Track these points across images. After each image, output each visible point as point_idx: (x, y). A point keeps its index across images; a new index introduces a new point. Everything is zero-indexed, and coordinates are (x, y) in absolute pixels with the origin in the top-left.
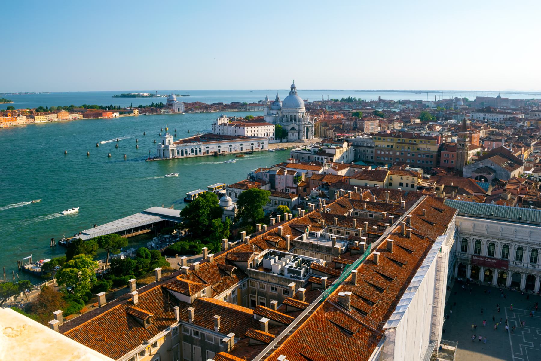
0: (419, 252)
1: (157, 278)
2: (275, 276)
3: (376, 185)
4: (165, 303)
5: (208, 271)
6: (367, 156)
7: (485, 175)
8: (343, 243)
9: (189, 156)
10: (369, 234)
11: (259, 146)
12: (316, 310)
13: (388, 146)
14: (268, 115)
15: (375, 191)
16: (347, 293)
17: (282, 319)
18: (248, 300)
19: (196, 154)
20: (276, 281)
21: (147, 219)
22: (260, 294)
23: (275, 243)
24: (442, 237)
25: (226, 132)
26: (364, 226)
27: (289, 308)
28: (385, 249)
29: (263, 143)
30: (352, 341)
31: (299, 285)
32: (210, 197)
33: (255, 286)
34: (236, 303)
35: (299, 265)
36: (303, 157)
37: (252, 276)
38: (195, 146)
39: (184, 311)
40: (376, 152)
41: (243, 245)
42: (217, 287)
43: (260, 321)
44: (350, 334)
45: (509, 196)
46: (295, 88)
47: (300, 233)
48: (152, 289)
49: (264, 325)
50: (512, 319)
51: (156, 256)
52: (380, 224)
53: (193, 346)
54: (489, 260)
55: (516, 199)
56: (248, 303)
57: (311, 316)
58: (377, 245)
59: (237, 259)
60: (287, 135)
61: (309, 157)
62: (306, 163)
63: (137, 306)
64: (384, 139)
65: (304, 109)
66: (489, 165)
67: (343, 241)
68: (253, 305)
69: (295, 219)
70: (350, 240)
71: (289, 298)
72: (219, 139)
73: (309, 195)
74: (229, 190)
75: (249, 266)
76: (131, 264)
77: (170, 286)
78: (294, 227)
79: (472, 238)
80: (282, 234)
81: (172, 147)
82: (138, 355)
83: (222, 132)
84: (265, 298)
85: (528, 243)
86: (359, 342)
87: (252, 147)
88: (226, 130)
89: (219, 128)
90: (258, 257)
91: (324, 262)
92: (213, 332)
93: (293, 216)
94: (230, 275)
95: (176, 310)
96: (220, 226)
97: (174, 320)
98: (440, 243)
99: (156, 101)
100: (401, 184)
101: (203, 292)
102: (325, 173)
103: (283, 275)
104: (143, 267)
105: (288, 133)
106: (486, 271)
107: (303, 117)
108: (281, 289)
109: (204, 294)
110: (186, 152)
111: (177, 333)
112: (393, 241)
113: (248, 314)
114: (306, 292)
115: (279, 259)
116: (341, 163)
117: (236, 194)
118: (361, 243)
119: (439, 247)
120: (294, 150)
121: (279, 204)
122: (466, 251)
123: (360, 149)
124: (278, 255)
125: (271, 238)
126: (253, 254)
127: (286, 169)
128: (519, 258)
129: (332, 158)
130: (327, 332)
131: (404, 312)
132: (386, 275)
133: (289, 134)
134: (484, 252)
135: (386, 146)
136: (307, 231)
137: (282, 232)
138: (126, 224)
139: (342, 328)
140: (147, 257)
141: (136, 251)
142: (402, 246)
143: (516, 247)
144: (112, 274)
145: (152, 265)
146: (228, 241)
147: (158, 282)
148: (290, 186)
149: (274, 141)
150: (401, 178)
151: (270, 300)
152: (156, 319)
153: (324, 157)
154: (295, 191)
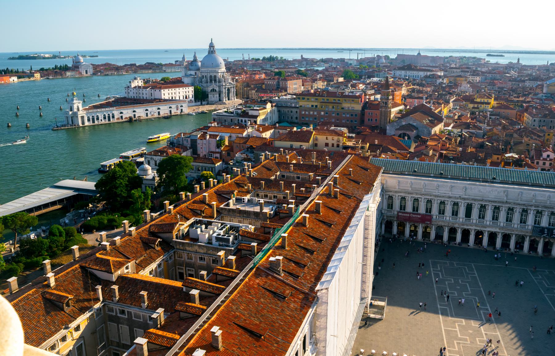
0: (347, 211)
1: (74, 257)
2: (203, 246)
3: (302, 146)
4: (85, 283)
5: (130, 246)
6: (292, 117)
7: (407, 133)
8: (271, 207)
9: (100, 122)
10: (297, 196)
11: (177, 109)
12: (248, 277)
13: (312, 106)
14: (186, 75)
15: (301, 152)
16: (278, 257)
17: (213, 289)
18: (176, 273)
19: (109, 120)
20: (205, 250)
21: (58, 194)
22: (189, 265)
23: (201, 211)
24: (369, 195)
25: (141, 95)
26: (291, 188)
27: (219, 278)
28: (314, 211)
29: (182, 106)
30: (285, 305)
31: (228, 253)
32: (128, 167)
33: (182, 258)
34: (163, 276)
35: (227, 232)
36: (225, 120)
37: (178, 247)
38: (107, 111)
39: (107, 290)
40: (300, 112)
41: (167, 215)
42: (141, 261)
43: (190, 293)
44: (283, 298)
45: (431, 152)
46: (213, 47)
47: (226, 199)
48: (69, 270)
49: (195, 297)
50: (436, 271)
51: (71, 234)
52: (307, 185)
53: (120, 325)
54: (414, 216)
55: (437, 155)
56: (176, 276)
57: (242, 284)
58: (306, 207)
59: (161, 231)
60: (208, 97)
61: (231, 119)
62: (229, 126)
63: (54, 289)
64: (308, 99)
65: (223, 69)
66: (411, 123)
67: (271, 205)
68: (181, 277)
69: (221, 185)
70: (278, 204)
71: (219, 267)
72: (134, 103)
73: (233, 159)
74: (148, 158)
75: (175, 237)
76: (44, 244)
77: (89, 265)
78: (220, 193)
79: (397, 195)
80: (207, 202)
81: (81, 113)
82: (59, 341)
83: (137, 95)
84: (194, 269)
85: (450, 197)
86: (292, 305)
87: (170, 111)
88: (141, 93)
89: (132, 91)
90: (184, 227)
91: (253, 227)
92: (140, 309)
93: (218, 183)
94: (154, 248)
95: (98, 289)
96: (140, 197)
97: (97, 300)
98: (368, 201)
99: (59, 63)
100: (327, 145)
101: (127, 268)
102: (249, 135)
103: (211, 243)
104: (57, 246)
105: (208, 95)
106: (411, 226)
108: (210, 259)
109: (127, 271)
110: (98, 119)
111: (101, 314)
112: (321, 202)
113: (177, 287)
114: (236, 260)
115: (206, 228)
116: (265, 125)
117: (156, 162)
118: (290, 206)
119: (366, 206)
120: (215, 112)
121: (202, 171)
122: (392, 208)
123: (284, 109)
124: (204, 224)
125: (196, 206)
126: (178, 224)
127: (208, 133)
128: (442, 212)
129: (255, 120)
130: (259, 299)
131: (335, 272)
132: (316, 237)
133: (210, 96)
134: (409, 208)
135: (310, 106)
136: (234, 197)
137: (207, 199)
138: (35, 201)
139: (274, 293)
140: (61, 235)
141: (48, 229)
142: (330, 206)
143: (439, 202)
144: (22, 256)
145: (67, 243)
146: (151, 212)
147: (75, 262)
148: (213, 151)
149: (194, 104)
150: (327, 139)
151: (199, 270)
152: (76, 301)
153: (247, 119)
154: (218, 155)
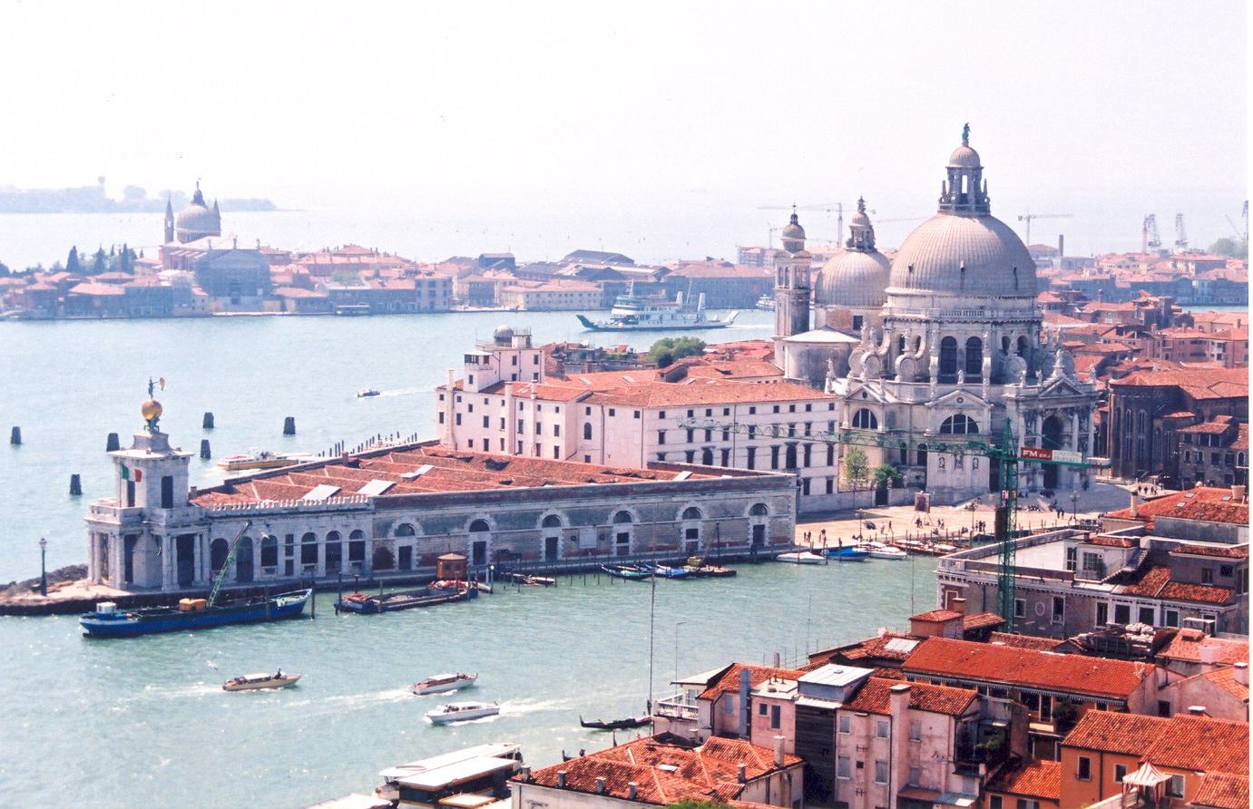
88: (529, 427)
107: (1029, 350)
